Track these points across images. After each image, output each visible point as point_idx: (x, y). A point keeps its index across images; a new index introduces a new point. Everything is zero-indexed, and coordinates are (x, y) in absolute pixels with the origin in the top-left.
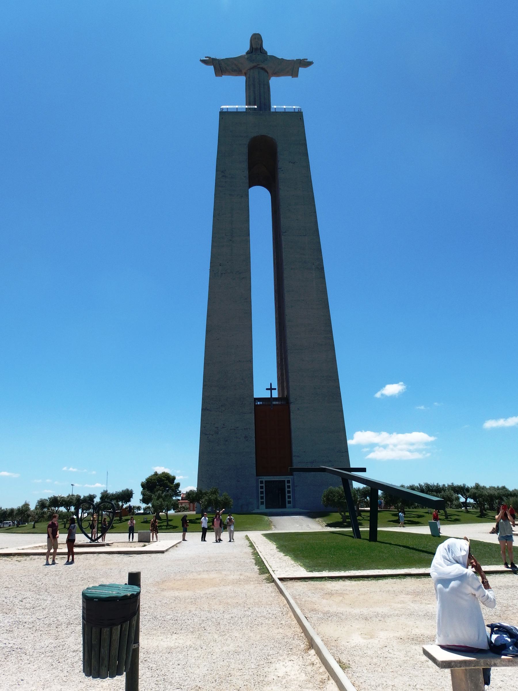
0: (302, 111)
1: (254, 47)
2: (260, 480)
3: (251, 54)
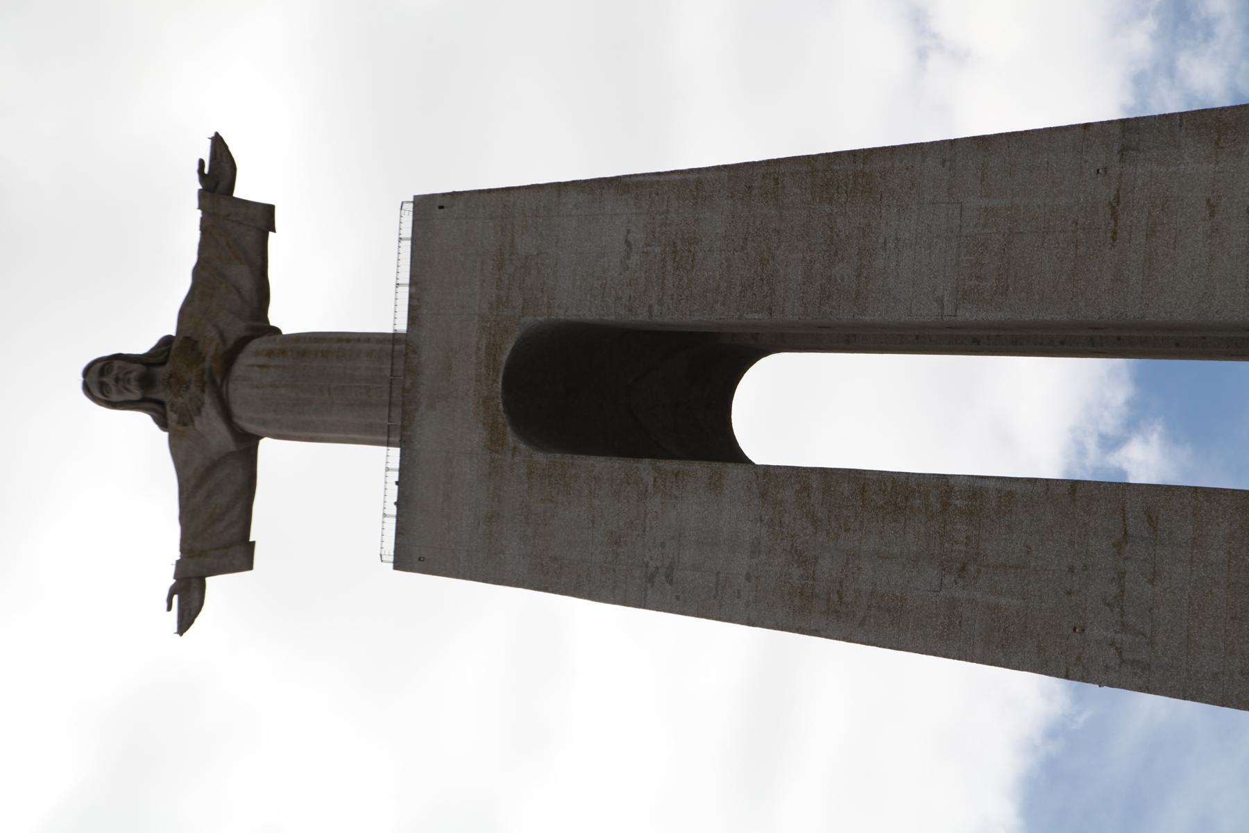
0: (412, 200)
1: (136, 395)
3: (168, 407)
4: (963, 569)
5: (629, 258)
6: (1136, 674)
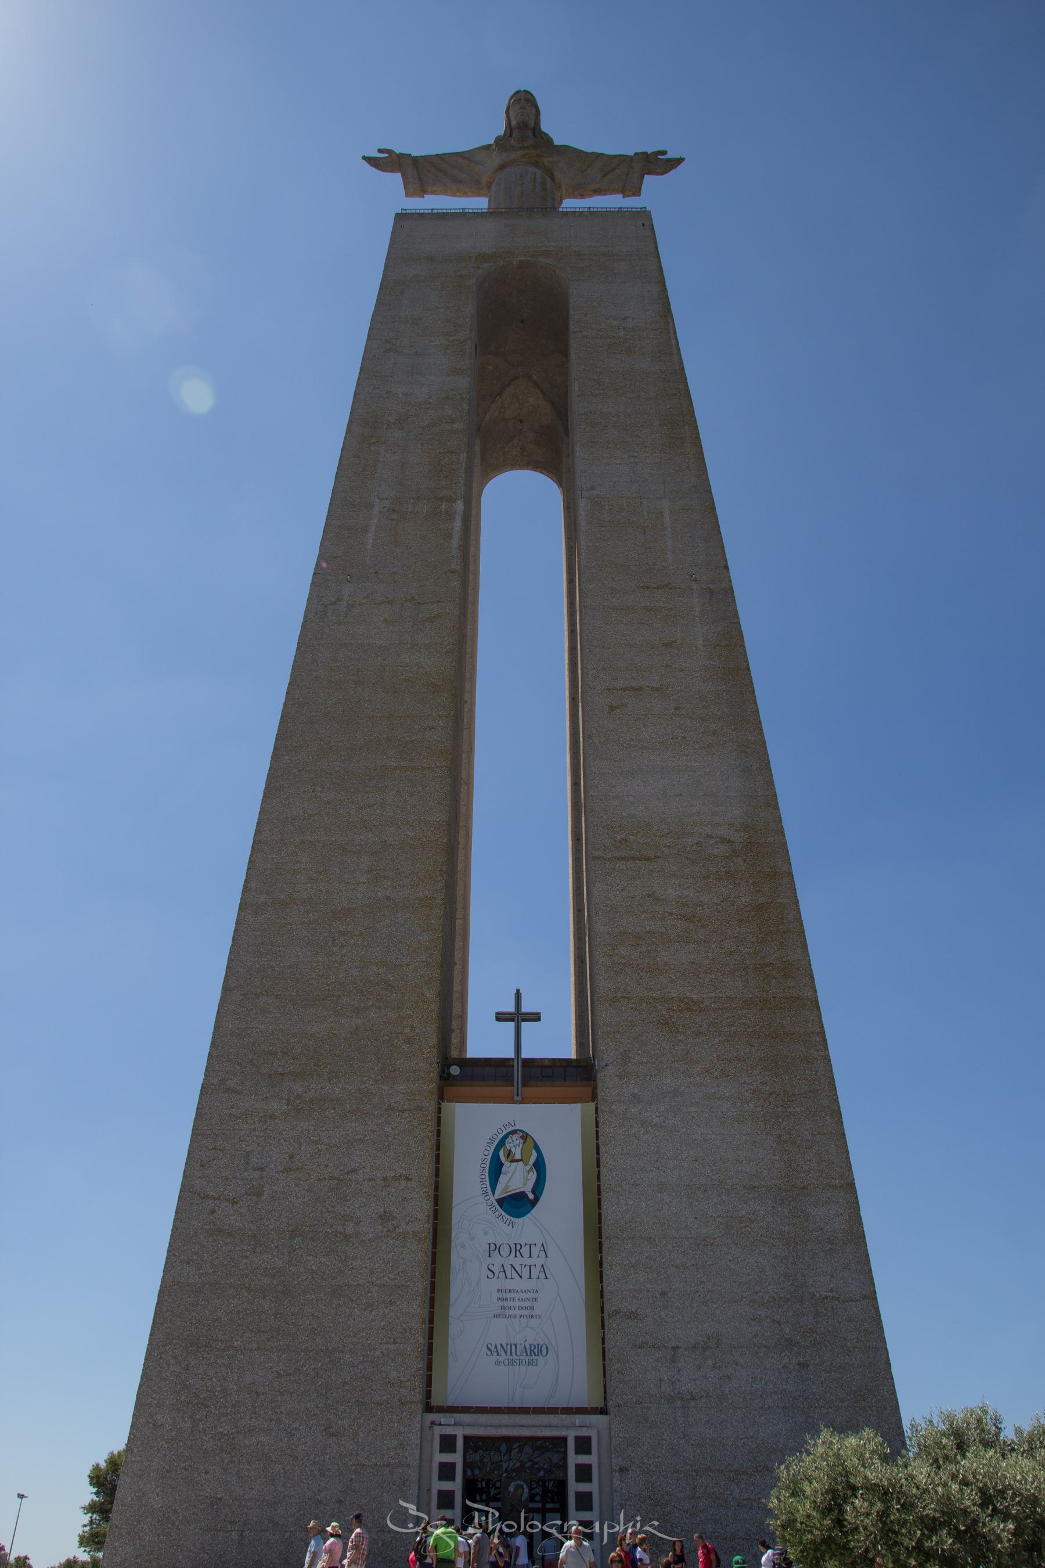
1: (514, 123)
2: (438, 1431)
6: (317, 614)
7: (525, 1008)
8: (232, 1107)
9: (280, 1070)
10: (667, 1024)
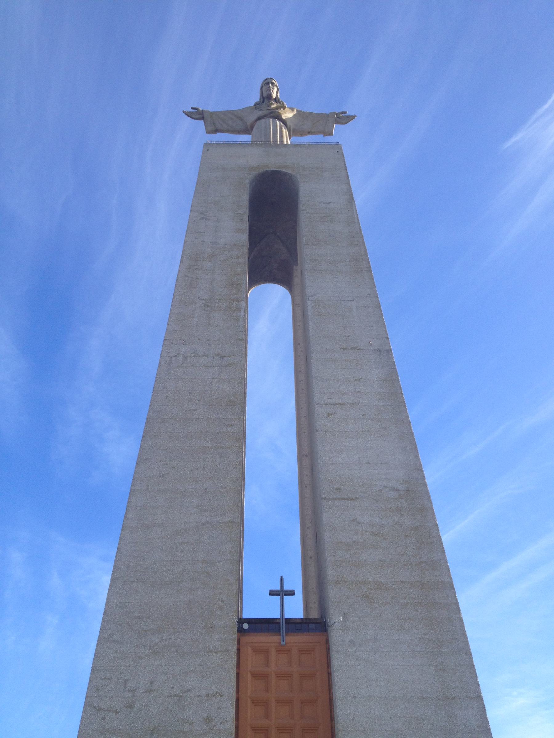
4: (208, 306)
5: (324, 203)
7: (286, 588)
8: (116, 652)
9: (145, 628)
10: (367, 597)
